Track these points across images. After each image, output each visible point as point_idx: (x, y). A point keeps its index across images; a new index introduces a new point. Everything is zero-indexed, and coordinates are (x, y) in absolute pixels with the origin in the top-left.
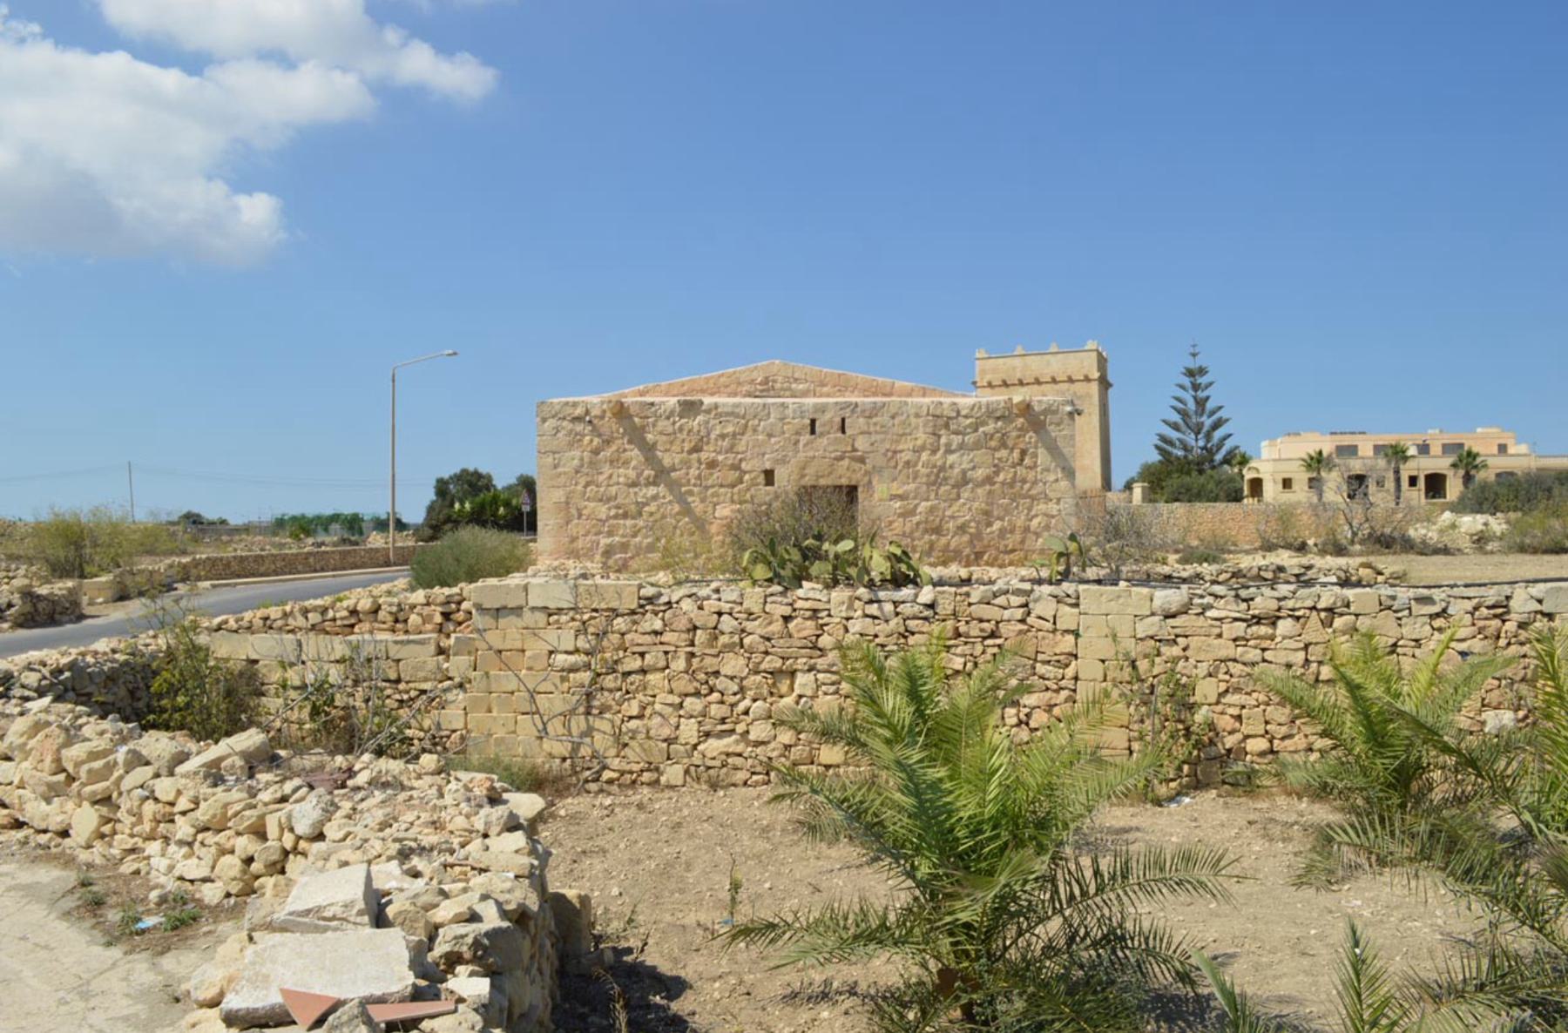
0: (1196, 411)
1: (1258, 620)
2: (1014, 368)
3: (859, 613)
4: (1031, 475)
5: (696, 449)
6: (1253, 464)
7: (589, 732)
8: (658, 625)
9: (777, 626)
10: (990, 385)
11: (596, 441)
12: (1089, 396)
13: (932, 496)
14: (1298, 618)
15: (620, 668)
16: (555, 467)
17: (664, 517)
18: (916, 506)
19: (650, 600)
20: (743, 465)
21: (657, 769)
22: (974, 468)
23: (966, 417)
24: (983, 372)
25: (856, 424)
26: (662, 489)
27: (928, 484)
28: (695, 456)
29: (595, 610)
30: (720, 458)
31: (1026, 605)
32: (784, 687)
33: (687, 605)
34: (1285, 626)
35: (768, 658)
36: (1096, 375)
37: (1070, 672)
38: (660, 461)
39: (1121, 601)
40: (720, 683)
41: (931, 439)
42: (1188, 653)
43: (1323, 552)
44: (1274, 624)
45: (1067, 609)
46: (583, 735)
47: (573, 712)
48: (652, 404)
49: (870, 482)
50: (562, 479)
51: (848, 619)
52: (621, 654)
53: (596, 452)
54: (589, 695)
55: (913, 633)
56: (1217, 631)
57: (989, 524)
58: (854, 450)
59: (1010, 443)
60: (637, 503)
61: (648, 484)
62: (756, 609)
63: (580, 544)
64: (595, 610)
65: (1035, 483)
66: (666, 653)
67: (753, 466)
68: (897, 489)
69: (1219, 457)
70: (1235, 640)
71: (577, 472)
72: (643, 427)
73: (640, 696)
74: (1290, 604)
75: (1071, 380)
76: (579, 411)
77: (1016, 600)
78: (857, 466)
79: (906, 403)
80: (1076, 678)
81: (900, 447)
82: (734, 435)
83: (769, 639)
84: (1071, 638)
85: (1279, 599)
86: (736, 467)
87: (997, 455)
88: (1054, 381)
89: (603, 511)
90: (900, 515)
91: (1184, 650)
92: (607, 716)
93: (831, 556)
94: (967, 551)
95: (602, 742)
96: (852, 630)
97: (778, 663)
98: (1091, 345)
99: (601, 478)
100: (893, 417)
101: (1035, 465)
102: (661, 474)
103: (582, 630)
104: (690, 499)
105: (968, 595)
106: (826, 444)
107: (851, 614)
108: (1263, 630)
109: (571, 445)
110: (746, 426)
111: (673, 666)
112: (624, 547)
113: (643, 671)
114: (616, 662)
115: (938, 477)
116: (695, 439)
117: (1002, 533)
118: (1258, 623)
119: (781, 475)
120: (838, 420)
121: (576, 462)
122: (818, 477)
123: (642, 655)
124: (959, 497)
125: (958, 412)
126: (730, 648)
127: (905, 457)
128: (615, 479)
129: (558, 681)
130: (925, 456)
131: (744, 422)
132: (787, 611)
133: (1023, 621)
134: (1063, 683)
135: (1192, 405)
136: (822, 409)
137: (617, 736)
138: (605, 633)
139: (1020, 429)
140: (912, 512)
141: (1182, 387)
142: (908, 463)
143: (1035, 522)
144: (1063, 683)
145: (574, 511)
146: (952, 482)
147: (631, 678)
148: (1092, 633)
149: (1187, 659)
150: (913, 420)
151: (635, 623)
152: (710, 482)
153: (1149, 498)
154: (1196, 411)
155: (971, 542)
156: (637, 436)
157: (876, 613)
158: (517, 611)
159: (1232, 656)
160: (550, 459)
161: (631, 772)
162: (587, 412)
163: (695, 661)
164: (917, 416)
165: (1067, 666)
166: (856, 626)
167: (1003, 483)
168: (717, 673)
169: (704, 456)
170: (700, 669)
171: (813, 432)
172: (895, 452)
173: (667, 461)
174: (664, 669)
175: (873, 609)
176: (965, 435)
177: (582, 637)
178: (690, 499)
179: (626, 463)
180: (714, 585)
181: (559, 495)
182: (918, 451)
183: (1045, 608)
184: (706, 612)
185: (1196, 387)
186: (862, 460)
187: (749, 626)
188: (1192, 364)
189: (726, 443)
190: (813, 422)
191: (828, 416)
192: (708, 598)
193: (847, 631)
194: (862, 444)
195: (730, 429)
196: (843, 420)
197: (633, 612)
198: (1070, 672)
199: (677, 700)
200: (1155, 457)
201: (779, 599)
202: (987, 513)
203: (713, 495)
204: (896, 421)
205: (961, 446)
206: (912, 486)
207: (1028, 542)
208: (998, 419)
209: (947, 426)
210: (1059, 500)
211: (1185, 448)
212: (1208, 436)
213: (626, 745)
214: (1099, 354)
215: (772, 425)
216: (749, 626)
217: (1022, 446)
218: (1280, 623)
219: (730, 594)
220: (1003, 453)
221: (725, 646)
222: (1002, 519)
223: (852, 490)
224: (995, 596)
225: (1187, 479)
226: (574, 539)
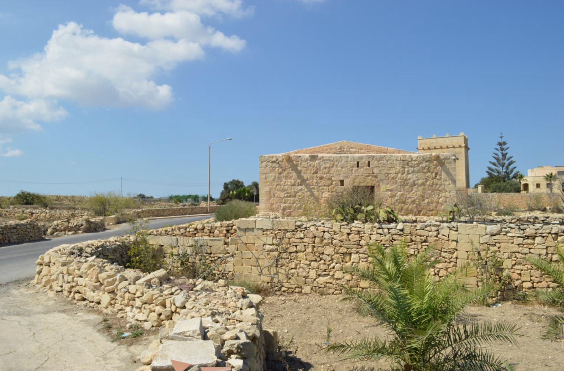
0: (503, 157)
1: (528, 237)
2: (433, 143)
3: (375, 232)
4: (439, 182)
5: (316, 173)
6: (524, 178)
7: (277, 273)
8: (302, 236)
9: (345, 237)
10: (423, 149)
11: (280, 170)
12: (461, 153)
13: (402, 190)
14: (543, 237)
15: (288, 251)
16: (266, 179)
17: (304, 197)
18: (396, 194)
19: (299, 227)
20: (333, 179)
21: (301, 287)
22: (418, 180)
23: (415, 161)
24: (421, 144)
25: (374, 164)
26: (303, 187)
27: (401, 186)
28: (315, 175)
29: (280, 230)
30: (324, 176)
31: (438, 230)
32: (347, 259)
33: (312, 229)
34: (538, 240)
35: (342, 248)
36: (464, 145)
37: (454, 255)
38: (303, 177)
39: (474, 229)
40: (324, 257)
41: (402, 169)
42: (500, 249)
43: (553, 212)
44: (534, 239)
45: (453, 232)
46: (275, 274)
47: (271, 266)
48: (300, 157)
49: (379, 185)
50: (268, 183)
51: (371, 234)
52: (289, 246)
53: (280, 174)
54: (277, 260)
55: (395, 240)
56: (512, 241)
57: (424, 200)
58: (373, 173)
59: (431, 170)
60: (294, 192)
61: (299, 185)
62: (337, 230)
63: (274, 206)
64: (280, 230)
65: (441, 185)
66: (305, 246)
67: (336, 178)
68: (388, 187)
69: (511, 176)
70: (518, 245)
71: (273, 181)
72: (297, 165)
73: (295, 261)
74: (540, 231)
75: (454, 147)
76: (274, 159)
77: (434, 229)
78: (374, 179)
79: (392, 156)
80: (457, 258)
81: (390, 172)
82: (329, 167)
83: (342, 241)
84: (455, 243)
85: (536, 230)
86: (330, 179)
87: (427, 175)
88: (448, 147)
89: (282, 195)
90: (390, 197)
91: (499, 248)
92: (284, 268)
93: (365, 211)
94: (415, 210)
95: (282, 277)
96: (372, 239)
97: (345, 250)
98: (462, 134)
99: (282, 183)
100: (388, 161)
101: (441, 179)
102: (303, 182)
103: (275, 236)
104: (313, 191)
105: (416, 226)
106: (362, 171)
107: (372, 233)
108: (530, 241)
109: (271, 171)
110: (334, 164)
111: (307, 250)
112: (290, 208)
113: (297, 252)
114: (287, 249)
115: (404, 183)
116: (315, 169)
117: (428, 203)
118: (528, 238)
119: (346, 182)
120: (367, 162)
121: (273, 177)
122: (360, 183)
123: (296, 246)
124: (412, 190)
125: (412, 159)
126: (328, 244)
127: (392, 175)
128: (287, 183)
129: (266, 255)
130: (399, 175)
131: (333, 163)
132: (349, 231)
133: (436, 236)
134: (452, 260)
135: (501, 156)
136: (361, 158)
137: (287, 275)
138: (283, 238)
139: (435, 165)
140: (395, 196)
141: (497, 149)
142: (393, 178)
143: (441, 200)
144: (452, 260)
145: (272, 195)
146: (409, 185)
147: (292, 254)
148: (462, 241)
149: (500, 251)
150: (395, 162)
151: (294, 235)
152: (320, 185)
153: (484, 191)
154: (503, 157)
155: (417, 207)
156: (294, 168)
157: (382, 233)
158: (252, 230)
159: (517, 251)
160: (264, 176)
161: (292, 288)
162: (277, 160)
163: (315, 249)
164: (397, 160)
165: (453, 253)
166: (374, 237)
167: (429, 185)
168: (323, 253)
169: (318, 175)
170: (317, 252)
171: (358, 166)
172: (388, 174)
173: (305, 177)
174: (304, 251)
175: (380, 231)
176: (414, 167)
177: (275, 239)
178: (313, 191)
179: (291, 177)
180: (322, 222)
181: (267, 189)
182: (397, 173)
183: (444, 230)
184: (319, 231)
185: (502, 149)
186: (376, 177)
187: (335, 236)
188: (501, 141)
189: (326, 170)
190: (358, 163)
191: (363, 161)
192: (320, 226)
193: (370, 239)
194: (376, 171)
195: (328, 165)
196: (369, 162)
197: (293, 231)
198: (454, 255)
199: (309, 263)
200: (486, 176)
201: (346, 227)
202: (423, 196)
203: (322, 189)
204: (389, 162)
205: (413, 172)
206: (394, 186)
207: (438, 207)
208: (427, 161)
209: (408, 164)
210: (450, 191)
211: (498, 172)
212: (507, 168)
213: (290, 278)
214: (465, 137)
215: (343, 164)
216: (335, 236)
217: (436, 171)
218: (537, 238)
219: (328, 225)
220: (429, 174)
221: (326, 243)
222: (428, 198)
223: (372, 188)
224: (426, 227)
225: (499, 184)
226: (272, 205)
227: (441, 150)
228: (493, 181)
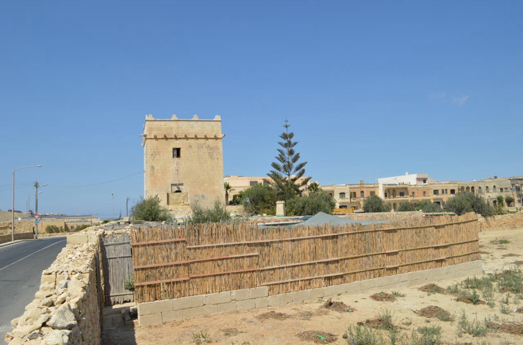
10: (156, 138)
75: (206, 138)
88: (196, 138)
98: (218, 118)
227: (185, 140)
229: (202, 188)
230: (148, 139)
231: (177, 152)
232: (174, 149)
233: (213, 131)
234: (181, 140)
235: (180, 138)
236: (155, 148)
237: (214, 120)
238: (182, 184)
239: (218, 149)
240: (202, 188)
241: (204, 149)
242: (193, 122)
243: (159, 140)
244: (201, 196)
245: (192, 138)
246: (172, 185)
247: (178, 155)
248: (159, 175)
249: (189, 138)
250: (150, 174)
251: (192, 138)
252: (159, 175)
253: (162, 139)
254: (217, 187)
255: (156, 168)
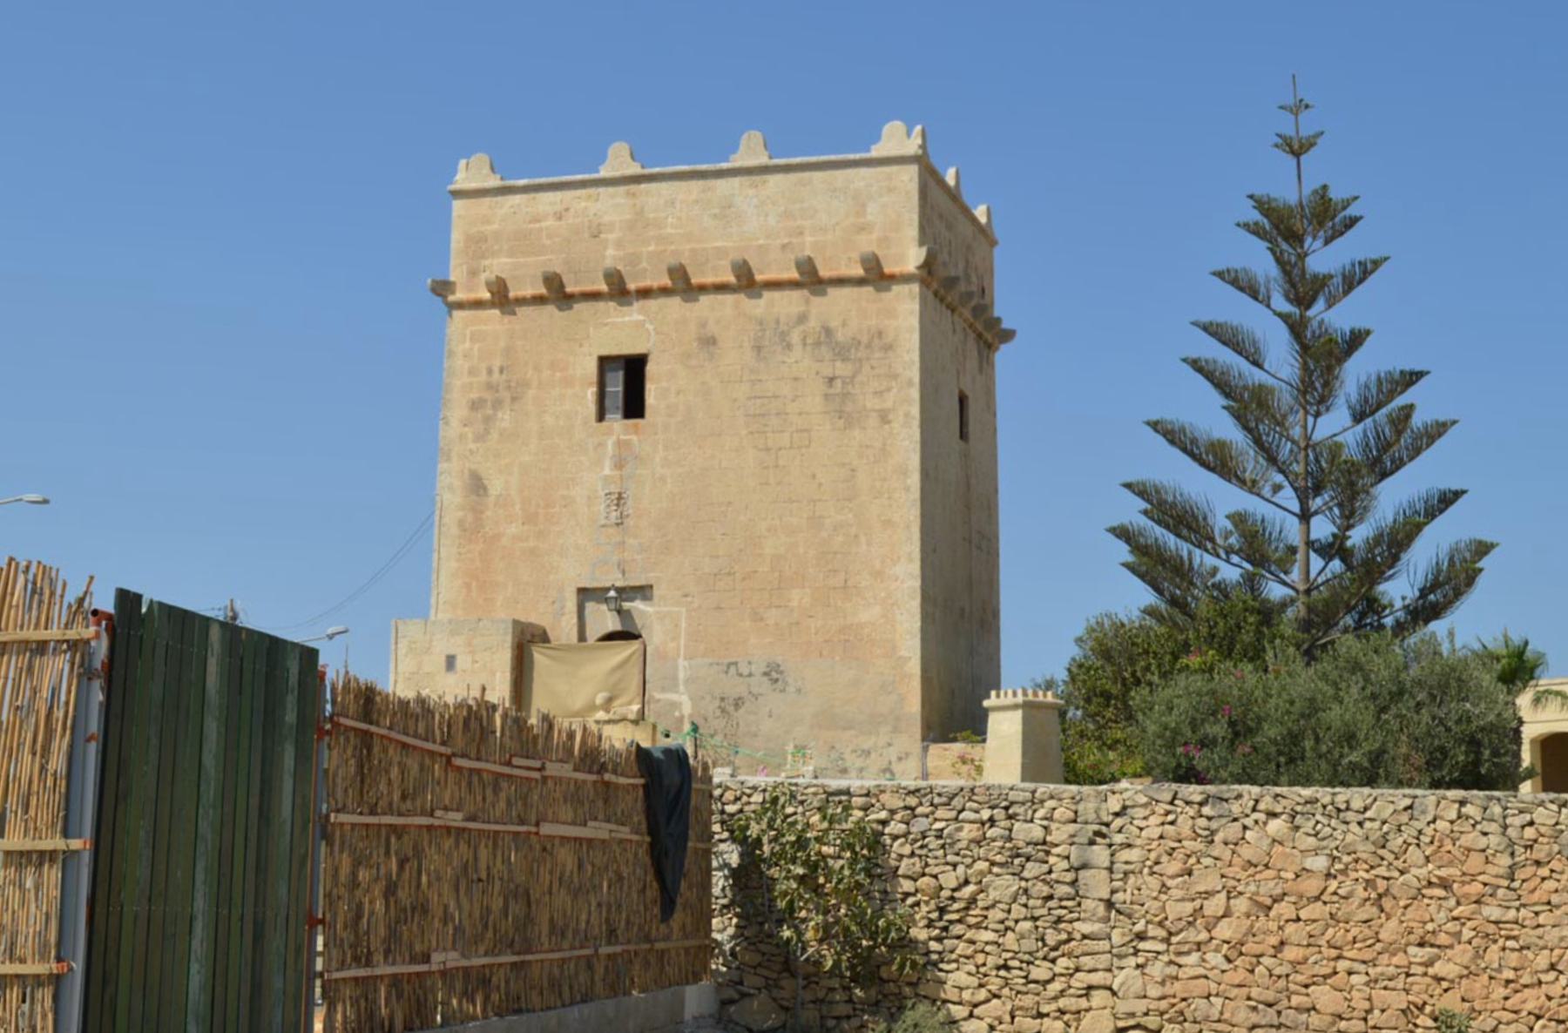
0: (1313, 400)
6: (1544, 683)
10: (501, 298)
12: (881, 342)
24: (479, 245)
36: (911, 257)
75: (811, 280)
98: (898, 139)
135: (1281, 362)
154: (1313, 400)
188: (1287, 191)
214: (930, 177)
225: (1238, 678)
227: (675, 302)
228: (1186, 648)
229: (772, 616)
230: (460, 305)
231: (626, 384)
232: (605, 362)
233: (862, 229)
234: (652, 304)
235: (645, 293)
236: (497, 364)
237: (876, 152)
238: (644, 592)
239: (888, 348)
240: (772, 616)
241: (798, 351)
242: (735, 182)
243: (523, 311)
244: (759, 668)
245: (721, 288)
246: (585, 594)
247: (634, 407)
248: (513, 529)
249: (703, 289)
250: (461, 523)
251: (721, 288)
252: (513, 529)
253: (539, 300)
254: (868, 614)
255: (495, 486)
